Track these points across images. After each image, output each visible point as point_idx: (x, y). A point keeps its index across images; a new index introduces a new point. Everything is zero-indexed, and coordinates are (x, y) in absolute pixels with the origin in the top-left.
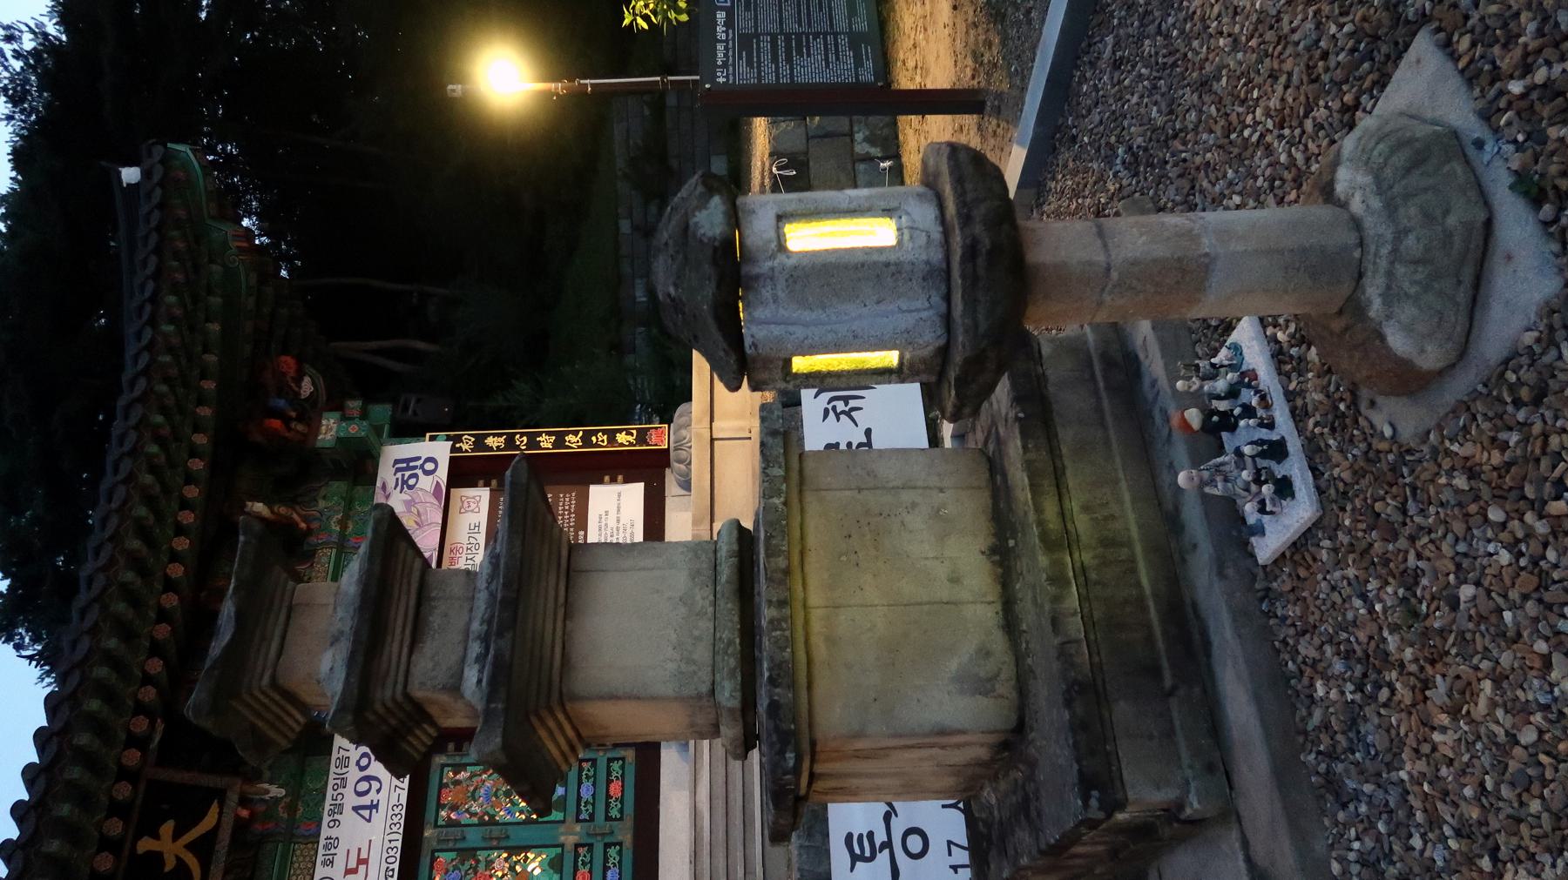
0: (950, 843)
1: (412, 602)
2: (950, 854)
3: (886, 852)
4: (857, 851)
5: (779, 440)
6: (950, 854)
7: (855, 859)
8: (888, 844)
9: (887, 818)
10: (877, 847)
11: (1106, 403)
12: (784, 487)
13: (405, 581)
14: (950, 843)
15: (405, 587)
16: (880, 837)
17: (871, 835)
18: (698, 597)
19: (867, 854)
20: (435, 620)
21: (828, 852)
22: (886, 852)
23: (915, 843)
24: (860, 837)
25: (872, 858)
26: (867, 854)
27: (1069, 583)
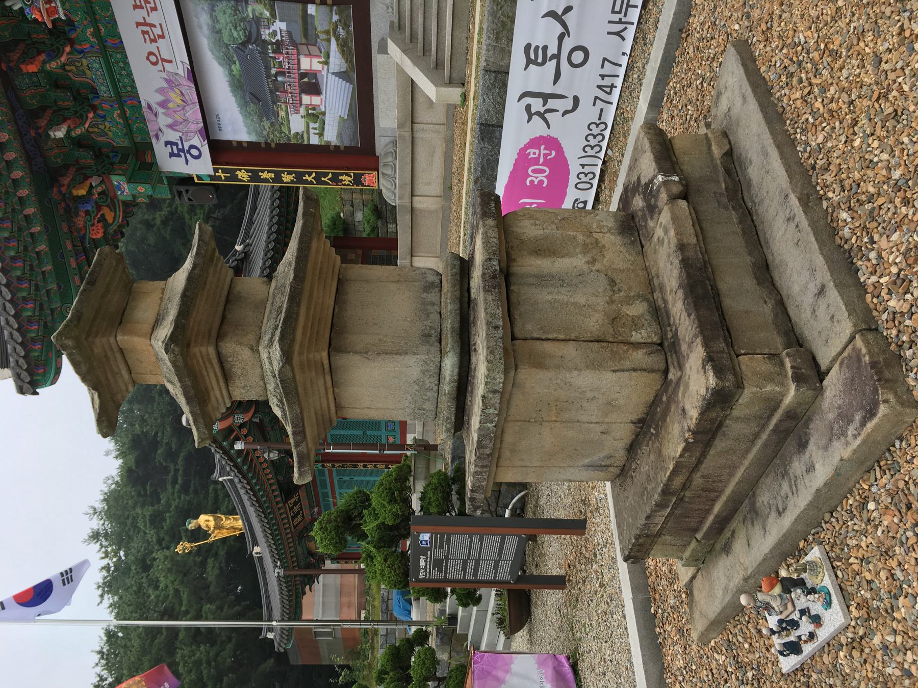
0: (605, 59)
1: (218, 369)
2: (602, 67)
3: (555, 61)
4: (532, 57)
5: (498, 395)
6: (602, 67)
7: (529, 62)
8: (557, 57)
9: (561, 38)
10: (549, 56)
11: (764, 436)
12: (496, 419)
13: (207, 363)
14: (605, 59)
15: (209, 366)
16: (553, 50)
17: (545, 48)
18: (427, 382)
19: (540, 60)
20: (237, 370)
21: (510, 52)
22: (555, 61)
23: (578, 57)
24: (537, 48)
25: (543, 63)
26: (540, 60)
27: (668, 507)
